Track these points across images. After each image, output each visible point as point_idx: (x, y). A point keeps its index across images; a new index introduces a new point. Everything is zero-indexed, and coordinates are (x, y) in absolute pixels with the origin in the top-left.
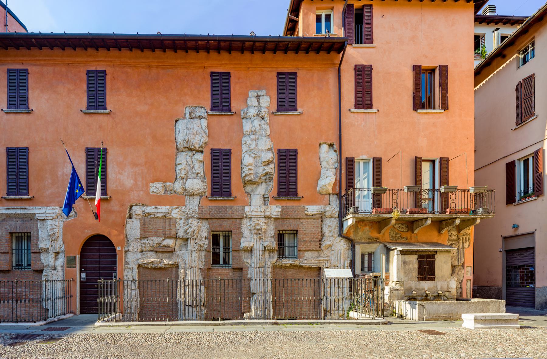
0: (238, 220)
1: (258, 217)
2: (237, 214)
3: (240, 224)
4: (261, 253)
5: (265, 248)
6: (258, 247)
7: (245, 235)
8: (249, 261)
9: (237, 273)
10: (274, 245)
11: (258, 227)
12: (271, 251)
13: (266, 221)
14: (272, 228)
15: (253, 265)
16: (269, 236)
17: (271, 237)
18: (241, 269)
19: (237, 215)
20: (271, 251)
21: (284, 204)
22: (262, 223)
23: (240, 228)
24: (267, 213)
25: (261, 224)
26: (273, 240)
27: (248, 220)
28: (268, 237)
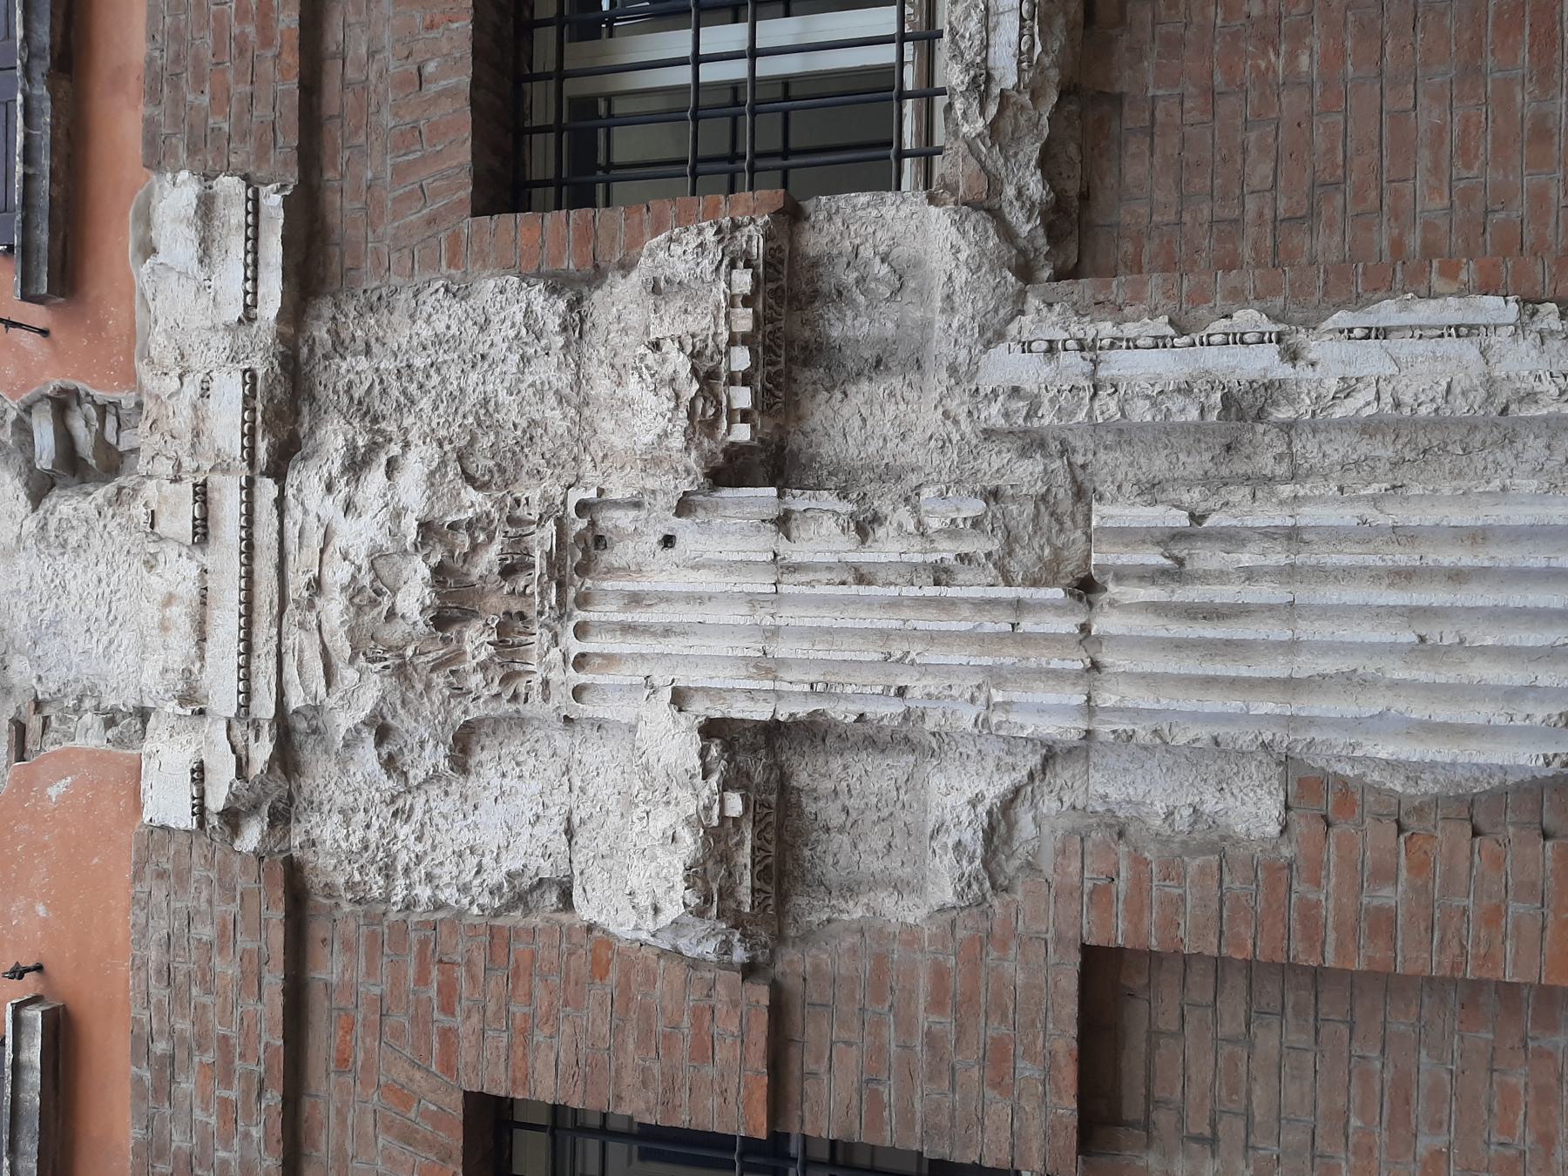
0: (329, 968)
1: (270, 599)
2: (227, 968)
3: (385, 931)
4: (823, 537)
5: (729, 471)
6: (712, 610)
7: (529, 850)
8: (957, 794)
9: (1185, 1054)
10: (677, 284)
11: (414, 595)
12: (791, 339)
13: (334, 437)
14: (445, 316)
15: (1048, 712)
16: (547, 371)
17: (576, 326)
18: (1105, 978)
19: (252, 980)
20: (791, 339)
21: (123, 121)
22: (353, 520)
23: (427, 939)
24: (226, 423)
25: (359, 535)
26: (619, 302)
27: (319, 772)
28: (577, 398)
